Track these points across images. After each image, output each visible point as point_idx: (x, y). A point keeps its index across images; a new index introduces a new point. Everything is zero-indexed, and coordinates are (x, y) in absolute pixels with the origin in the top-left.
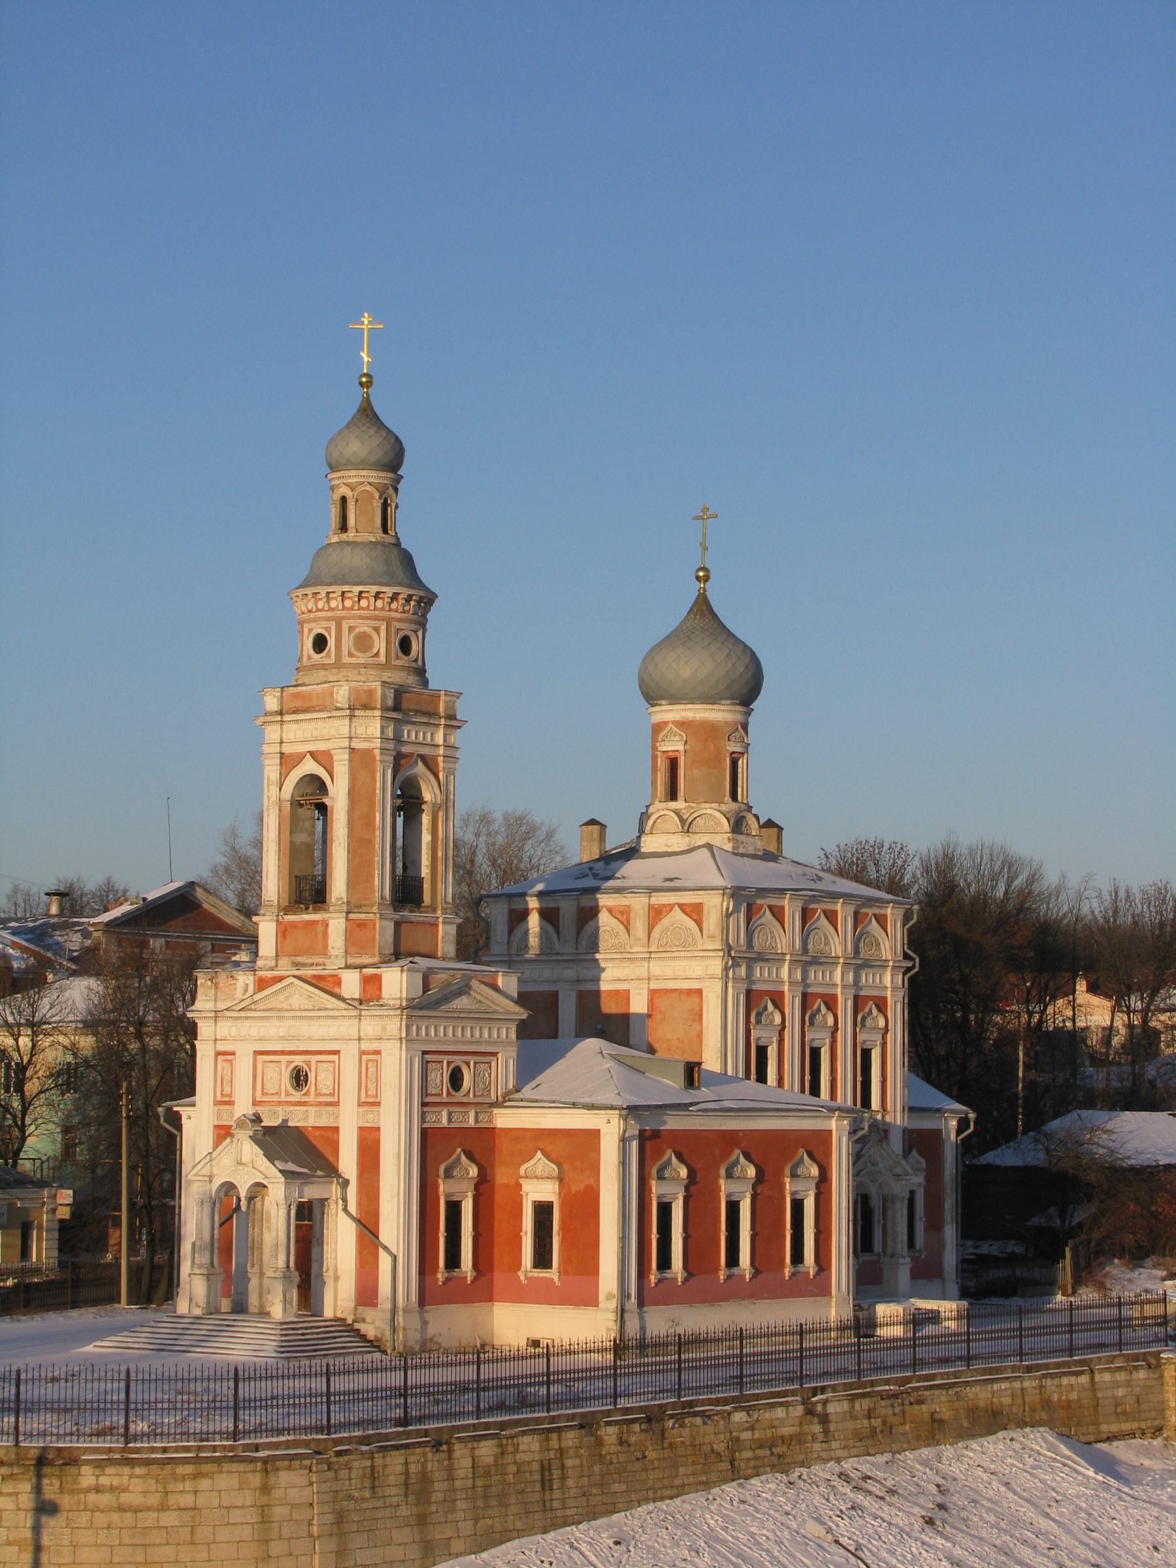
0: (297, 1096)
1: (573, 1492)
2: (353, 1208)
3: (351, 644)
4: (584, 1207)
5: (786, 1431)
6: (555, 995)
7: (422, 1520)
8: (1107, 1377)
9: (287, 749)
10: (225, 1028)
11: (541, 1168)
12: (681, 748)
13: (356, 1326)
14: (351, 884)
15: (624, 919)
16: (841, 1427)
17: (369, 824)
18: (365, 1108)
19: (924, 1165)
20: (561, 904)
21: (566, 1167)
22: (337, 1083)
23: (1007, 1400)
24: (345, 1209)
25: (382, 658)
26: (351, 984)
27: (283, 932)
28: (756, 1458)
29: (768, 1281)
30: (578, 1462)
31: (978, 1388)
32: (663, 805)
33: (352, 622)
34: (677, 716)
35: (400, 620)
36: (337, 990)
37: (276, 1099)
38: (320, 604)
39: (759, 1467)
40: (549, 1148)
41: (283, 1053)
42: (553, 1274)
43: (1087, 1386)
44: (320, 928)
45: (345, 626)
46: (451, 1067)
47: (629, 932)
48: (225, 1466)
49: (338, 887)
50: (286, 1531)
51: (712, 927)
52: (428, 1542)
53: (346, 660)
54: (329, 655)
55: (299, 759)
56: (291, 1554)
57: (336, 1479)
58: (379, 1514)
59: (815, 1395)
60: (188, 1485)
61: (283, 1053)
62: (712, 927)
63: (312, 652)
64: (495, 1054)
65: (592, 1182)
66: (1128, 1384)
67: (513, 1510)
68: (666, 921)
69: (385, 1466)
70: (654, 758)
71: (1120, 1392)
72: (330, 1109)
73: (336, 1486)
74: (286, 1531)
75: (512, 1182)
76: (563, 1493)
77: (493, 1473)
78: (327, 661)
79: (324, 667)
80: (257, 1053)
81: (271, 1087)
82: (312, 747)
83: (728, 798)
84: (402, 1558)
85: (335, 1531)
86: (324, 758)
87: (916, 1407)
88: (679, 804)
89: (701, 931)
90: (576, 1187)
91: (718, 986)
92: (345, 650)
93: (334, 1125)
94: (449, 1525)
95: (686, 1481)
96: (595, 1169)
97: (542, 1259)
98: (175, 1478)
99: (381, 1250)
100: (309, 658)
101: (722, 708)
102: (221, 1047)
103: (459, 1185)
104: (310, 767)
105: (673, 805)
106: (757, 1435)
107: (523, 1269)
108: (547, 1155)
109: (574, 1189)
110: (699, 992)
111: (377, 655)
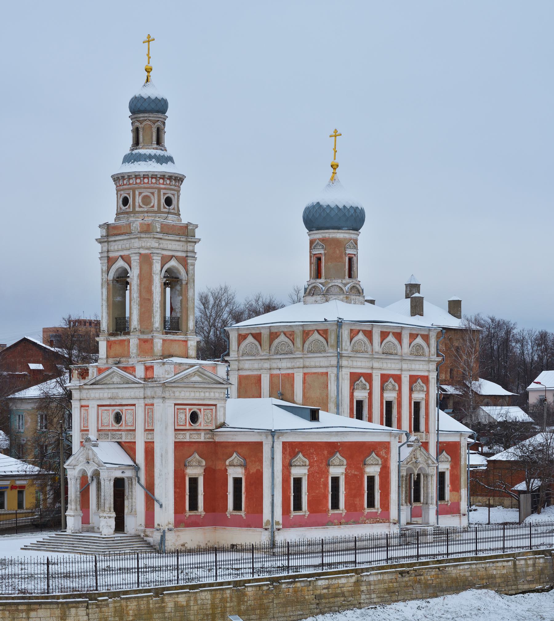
0: (117, 427)
2: (143, 481)
3: (140, 201)
4: (256, 480)
6: (260, 376)
9: (111, 255)
10: (84, 394)
11: (236, 461)
12: (322, 252)
13: (145, 538)
15: (291, 338)
16: (377, 587)
18: (147, 432)
19: (450, 459)
20: (262, 331)
21: (248, 460)
22: (135, 420)
23: (468, 574)
24: (138, 482)
25: (156, 208)
26: (140, 371)
27: (110, 345)
29: (354, 516)
32: (314, 281)
33: (141, 191)
34: (320, 236)
35: (165, 189)
36: (134, 373)
37: (107, 428)
38: (125, 182)
39: (331, 607)
40: (240, 451)
41: (110, 406)
42: (243, 513)
43: (512, 567)
44: (126, 343)
45: (137, 193)
47: (293, 344)
48: (43, 606)
49: (135, 323)
51: (332, 342)
53: (137, 209)
54: (129, 208)
55: (116, 259)
59: (362, 572)
60: (24, 615)
61: (110, 406)
62: (332, 342)
63: (122, 206)
64: (215, 405)
65: (259, 468)
68: (311, 339)
69: (127, 606)
70: (311, 257)
72: (131, 432)
75: (223, 469)
78: (128, 210)
79: (127, 213)
80: (99, 406)
81: (105, 421)
82: (122, 253)
83: (347, 277)
86: (127, 259)
88: (322, 280)
89: (327, 342)
90: (253, 470)
92: (137, 204)
93: (133, 441)
95: (291, 614)
96: (261, 461)
97: (237, 506)
98: (17, 610)
99: (155, 502)
100: (121, 209)
101: (343, 231)
102: (84, 403)
103: (196, 470)
104: (121, 263)
105: (319, 281)
107: (228, 511)
108: (238, 454)
109: (251, 472)
110: (327, 373)
111: (153, 207)
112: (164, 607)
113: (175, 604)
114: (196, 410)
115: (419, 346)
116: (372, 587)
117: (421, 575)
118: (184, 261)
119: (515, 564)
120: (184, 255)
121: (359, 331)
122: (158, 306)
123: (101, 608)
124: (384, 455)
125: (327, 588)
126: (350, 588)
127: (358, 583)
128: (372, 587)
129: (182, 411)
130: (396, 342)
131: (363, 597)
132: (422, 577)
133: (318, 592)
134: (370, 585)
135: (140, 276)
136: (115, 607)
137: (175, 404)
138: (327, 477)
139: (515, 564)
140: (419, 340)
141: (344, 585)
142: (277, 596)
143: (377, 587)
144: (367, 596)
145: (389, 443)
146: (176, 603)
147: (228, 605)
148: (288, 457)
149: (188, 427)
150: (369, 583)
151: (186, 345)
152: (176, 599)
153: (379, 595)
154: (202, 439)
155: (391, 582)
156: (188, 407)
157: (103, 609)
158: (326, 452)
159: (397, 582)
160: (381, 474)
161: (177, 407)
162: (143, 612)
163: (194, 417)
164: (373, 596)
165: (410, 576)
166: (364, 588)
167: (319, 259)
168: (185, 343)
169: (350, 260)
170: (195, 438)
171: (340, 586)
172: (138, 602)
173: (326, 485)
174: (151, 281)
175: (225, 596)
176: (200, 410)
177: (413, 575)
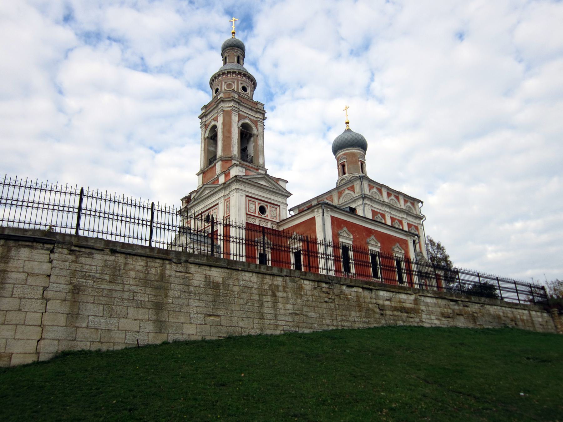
1: (282, 312)
5: (408, 305)
7: (159, 307)
14: (224, 150)
16: (434, 309)
17: (230, 132)
23: (501, 314)
28: (395, 316)
30: (285, 295)
33: (225, 81)
45: (223, 83)
46: (260, 205)
49: (220, 153)
50: (18, 291)
52: (161, 321)
56: (20, 310)
57: (75, 262)
58: (118, 295)
64: (279, 206)
66: (542, 317)
67: (237, 314)
69: (126, 264)
71: (540, 320)
73: (78, 267)
74: (18, 291)
76: (275, 310)
77: (221, 287)
82: (213, 118)
84: (137, 329)
85: (69, 297)
87: (466, 308)
88: (347, 175)
91: (362, 207)
94: (182, 314)
104: (213, 123)
106: (393, 305)
112: (188, 278)
113: (206, 277)
114: (263, 205)
115: (409, 207)
117: (467, 306)
118: (256, 123)
119: (530, 313)
120: (256, 119)
122: (236, 141)
123: (77, 257)
125: (389, 300)
129: (252, 202)
130: (396, 201)
132: (469, 309)
135: (224, 124)
136: (106, 261)
137: (247, 196)
139: (530, 313)
140: (409, 204)
144: (428, 317)
146: (207, 277)
147: (280, 294)
148: (336, 228)
149: (257, 215)
150: (427, 305)
152: (208, 272)
153: (437, 317)
154: (269, 226)
156: (257, 202)
157: (82, 260)
158: (364, 234)
162: (152, 277)
163: (262, 210)
164: (433, 317)
166: (423, 308)
167: (343, 166)
169: (362, 164)
170: (263, 224)
171: (402, 301)
172: (147, 263)
174: (230, 126)
175: (275, 283)
176: (267, 206)
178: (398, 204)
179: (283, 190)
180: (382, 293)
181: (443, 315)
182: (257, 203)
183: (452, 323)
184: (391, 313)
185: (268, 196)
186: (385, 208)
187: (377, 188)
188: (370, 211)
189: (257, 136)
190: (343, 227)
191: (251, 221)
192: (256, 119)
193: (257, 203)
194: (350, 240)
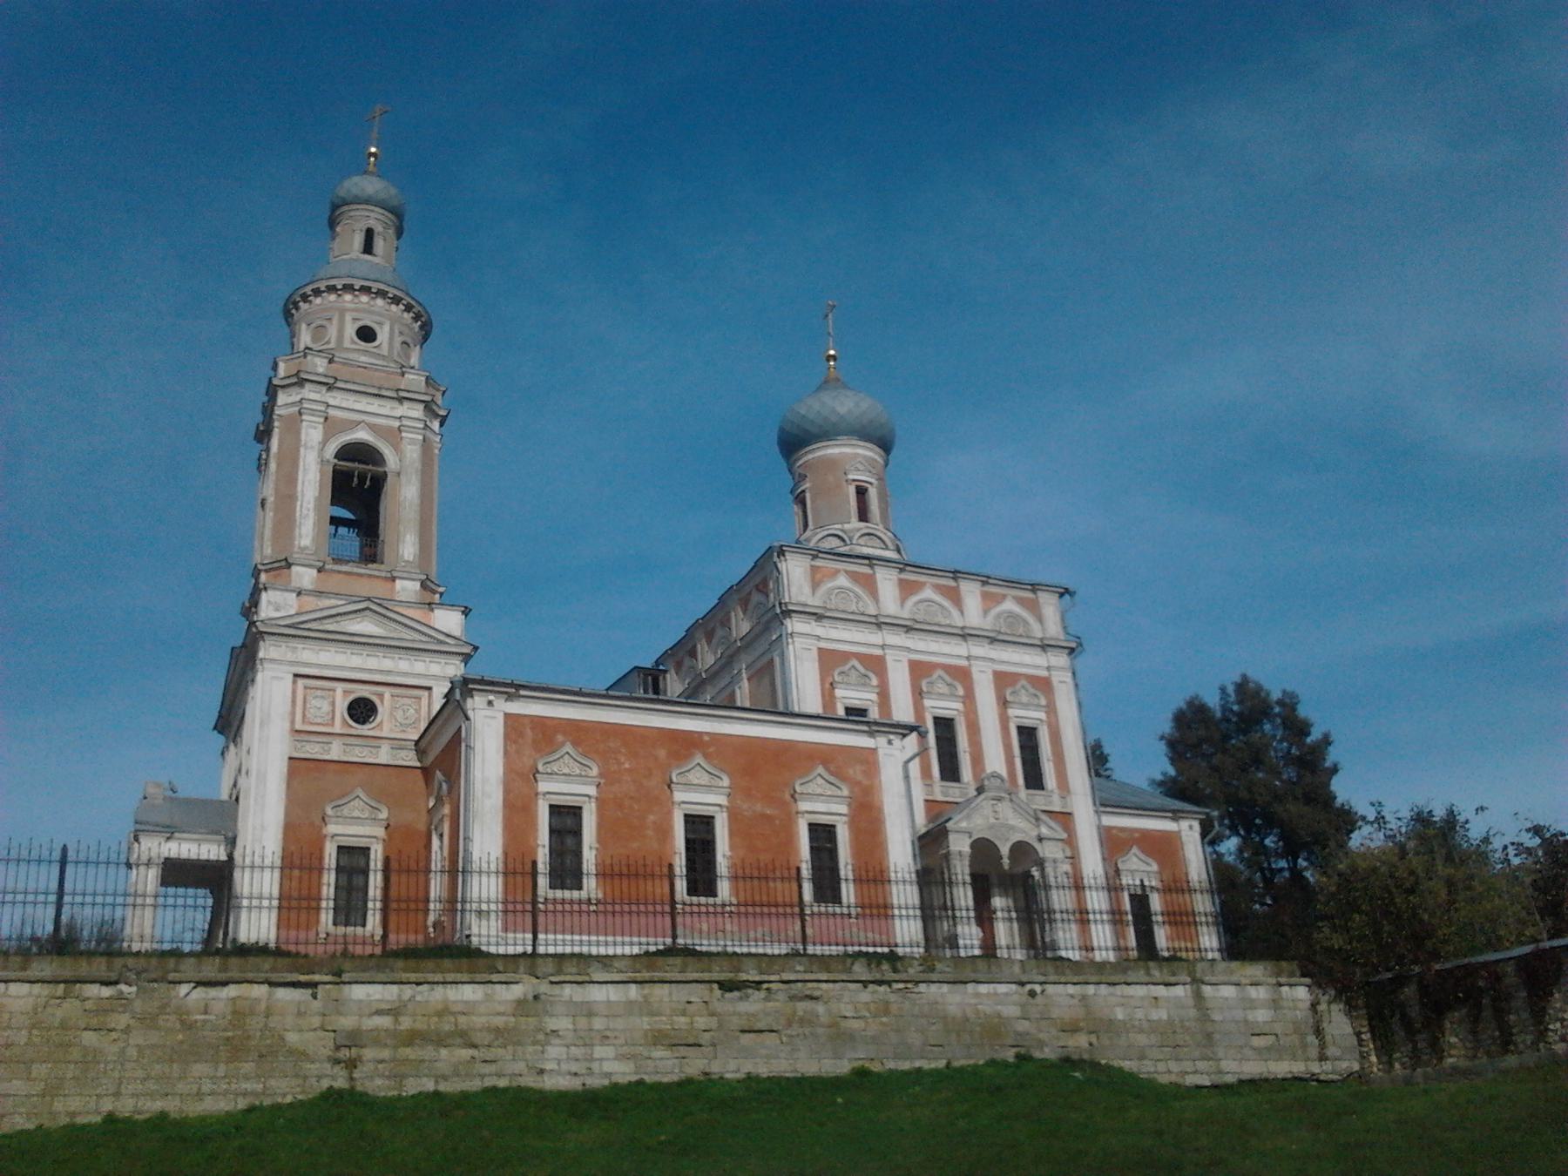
8: (1228, 992)
23: (1011, 1011)
31: (945, 988)
46: (352, 697)
64: (429, 689)
71: (1261, 1015)
114: (366, 695)
115: (1011, 615)
116: (598, 1024)
121: (838, 571)
124: (860, 777)
126: (499, 1021)
127: (529, 1006)
128: (598, 1024)
129: (319, 693)
130: (946, 603)
131: (555, 1051)
132: (820, 1008)
133: (347, 1022)
134: (590, 1014)
137: (296, 676)
138: (670, 813)
140: (1009, 605)
141: (469, 1009)
142: (148, 1021)
143: (619, 1024)
145: (874, 751)
149: (338, 728)
151: (393, 588)
153: (626, 1049)
155: (684, 1013)
156: (340, 687)
158: (662, 753)
159: (712, 1014)
160: (854, 823)
161: (301, 682)
163: (362, 710)
164: (599, 1052)
165: (767, 999)
166: (562, 1023)
168: (389, 585)
171: (455, 1008)
173: (665, 832)
176: (381, 696)
177: (781, 996)
178: (955, 612)
179: (442, 637)
180: (359, 992)
181: (657, 1038)
182: (339, 692)
183: (695, 1065)
184: (386, 1054)
185: (387, 664)
186: (876, 637)
187: (854, 576)
188: (815, 653)
189: (399, 474)
190: (563, 744)
191: (313, 750)
192: (397, 424)
193: (339, 692)
194: (590, 784)
